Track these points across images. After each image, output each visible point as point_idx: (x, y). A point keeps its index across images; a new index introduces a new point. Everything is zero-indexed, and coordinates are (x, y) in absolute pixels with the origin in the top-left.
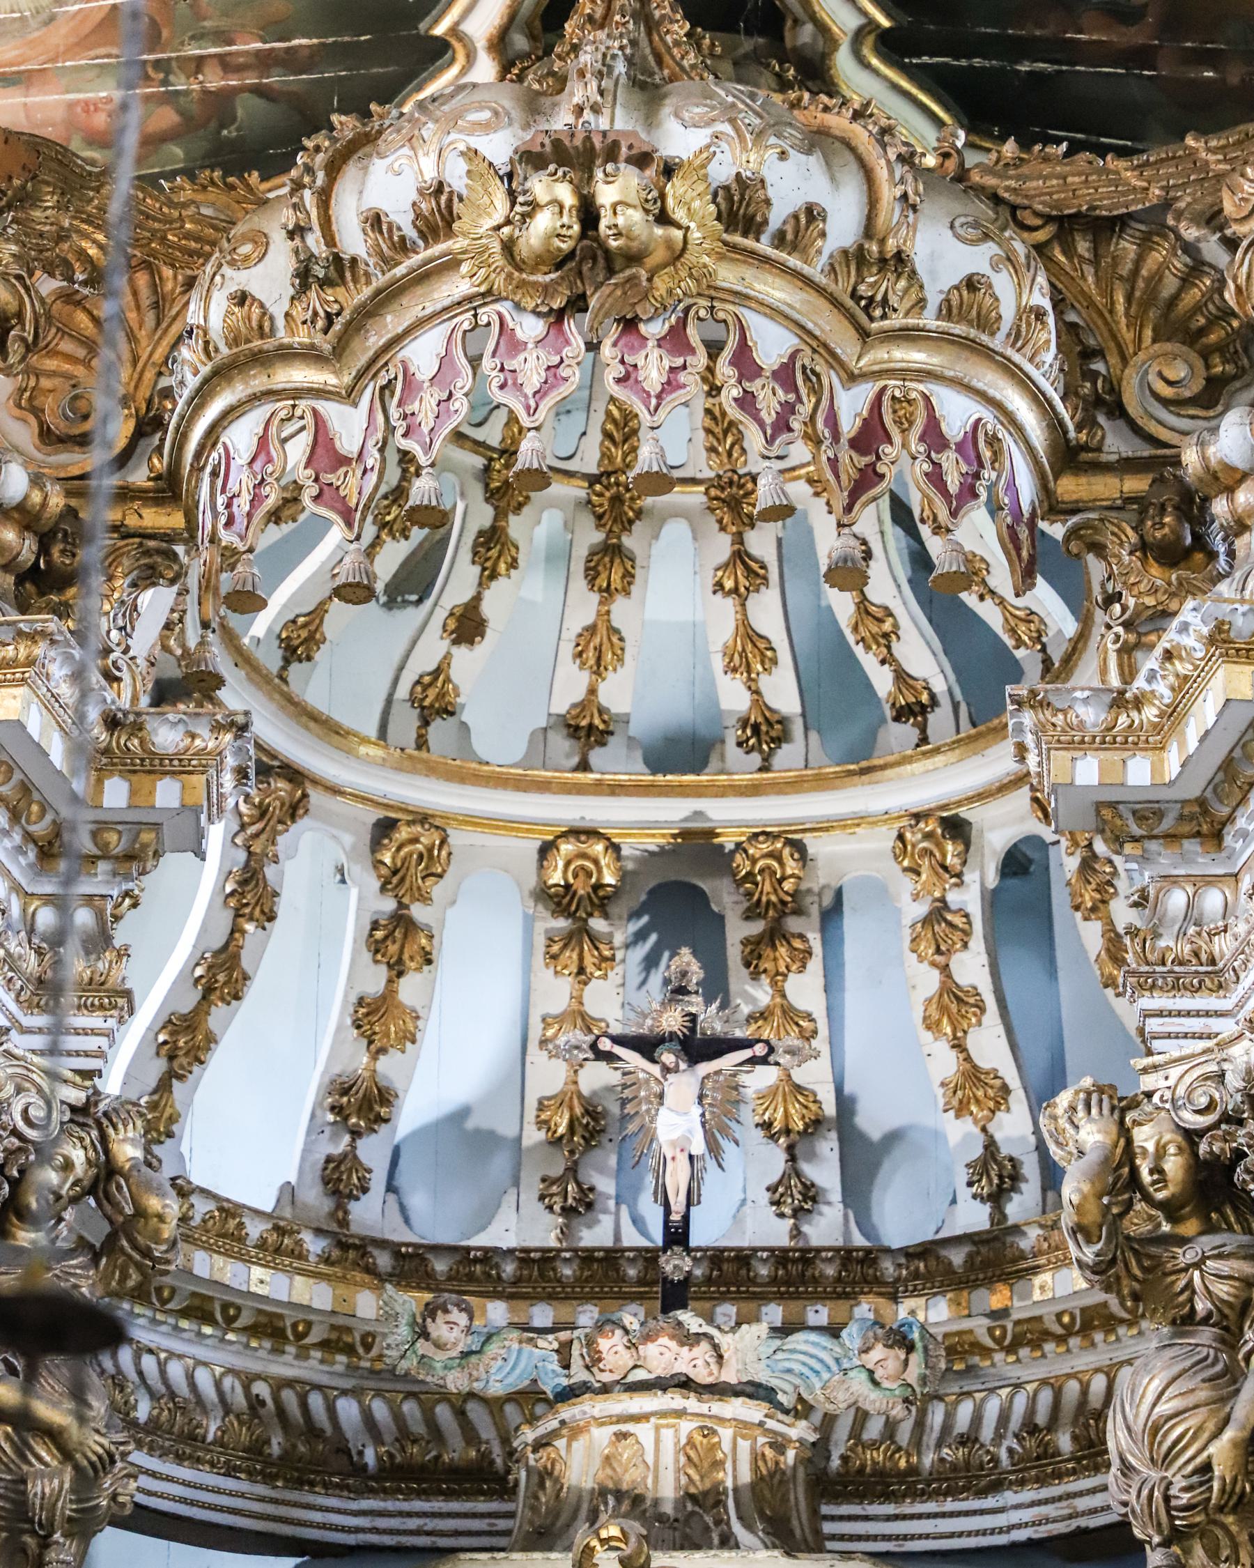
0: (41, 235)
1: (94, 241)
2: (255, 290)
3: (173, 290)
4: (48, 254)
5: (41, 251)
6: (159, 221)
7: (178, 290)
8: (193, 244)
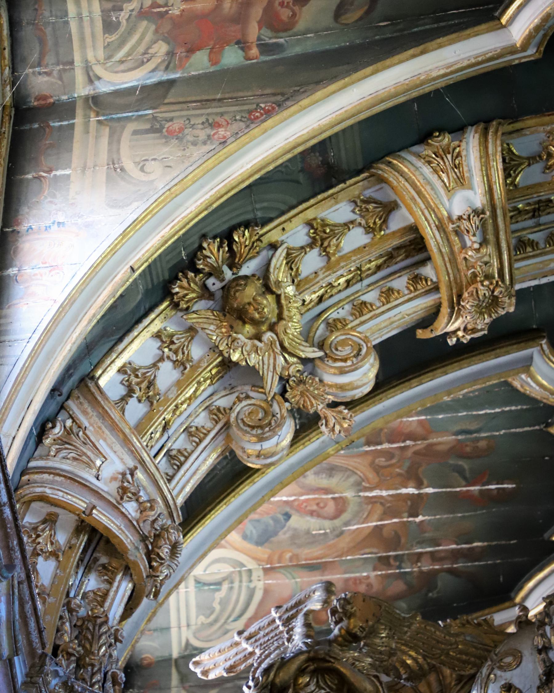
0: (381, 653)
1: (410, 656)
2: (516, 682)
3: (450, 683)
4: (385, 663)
5: (382, 662)
6: (445, 644)
7: (453, 684)
8: (464, 657)
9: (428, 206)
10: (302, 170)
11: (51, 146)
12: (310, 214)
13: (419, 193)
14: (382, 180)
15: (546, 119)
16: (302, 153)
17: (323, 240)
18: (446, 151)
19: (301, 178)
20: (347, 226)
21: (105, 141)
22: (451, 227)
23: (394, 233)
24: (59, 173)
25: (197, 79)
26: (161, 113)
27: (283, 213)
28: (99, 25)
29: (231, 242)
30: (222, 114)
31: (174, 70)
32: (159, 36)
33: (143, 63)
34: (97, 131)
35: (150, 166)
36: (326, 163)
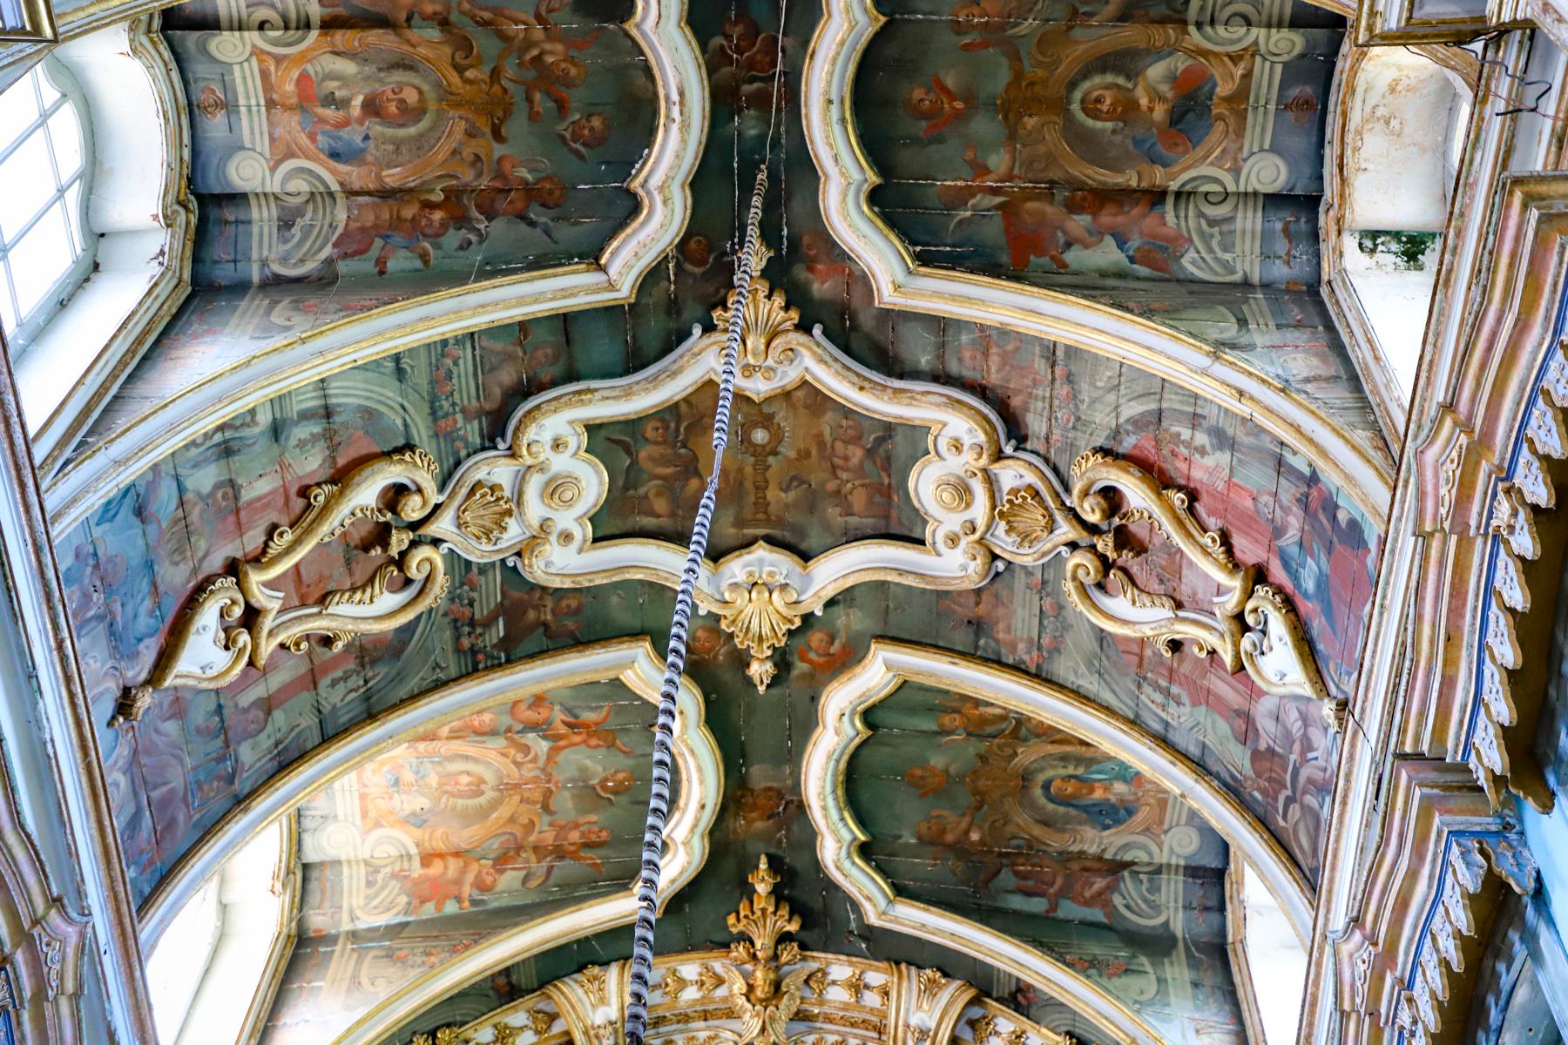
9: (578, 1017)
10: (492, 988)
11: (316, 965)
12: (496, 1020)
13: (573, 1007)
14: (549, 997)
15: (666, 959)
16: (493, 976)
17: (503, 1038)
18: (595, 978)
19: (491, 993)
20: (522, 1028)
21: (352, 963)
22: (592, 1033)
23: (554, 1036)
24: (314, 984)
25: (425, 922)
26: (396, 944)
27: (477, 1018)
28: (363, 882)
29: (434, 1037)
30: (435, 947)
31: (410, 915)
32: (402, 891)
33: (389, 909)
34: (350, 956)
35: (380, 981)
36: (509, 983)
